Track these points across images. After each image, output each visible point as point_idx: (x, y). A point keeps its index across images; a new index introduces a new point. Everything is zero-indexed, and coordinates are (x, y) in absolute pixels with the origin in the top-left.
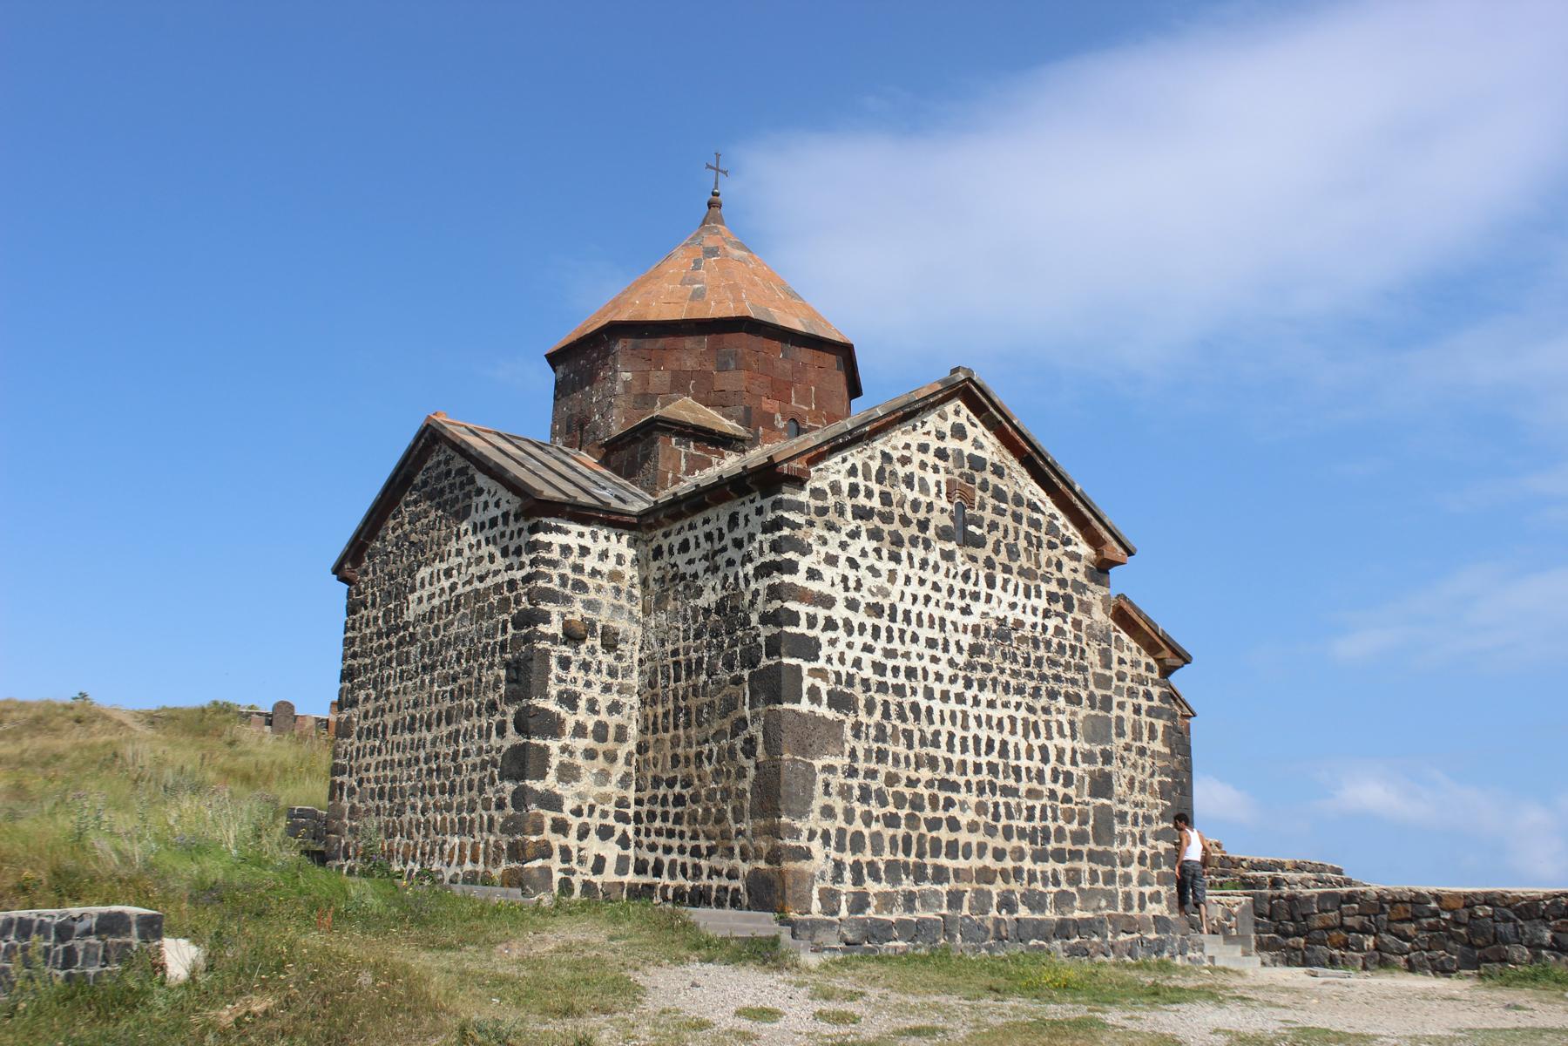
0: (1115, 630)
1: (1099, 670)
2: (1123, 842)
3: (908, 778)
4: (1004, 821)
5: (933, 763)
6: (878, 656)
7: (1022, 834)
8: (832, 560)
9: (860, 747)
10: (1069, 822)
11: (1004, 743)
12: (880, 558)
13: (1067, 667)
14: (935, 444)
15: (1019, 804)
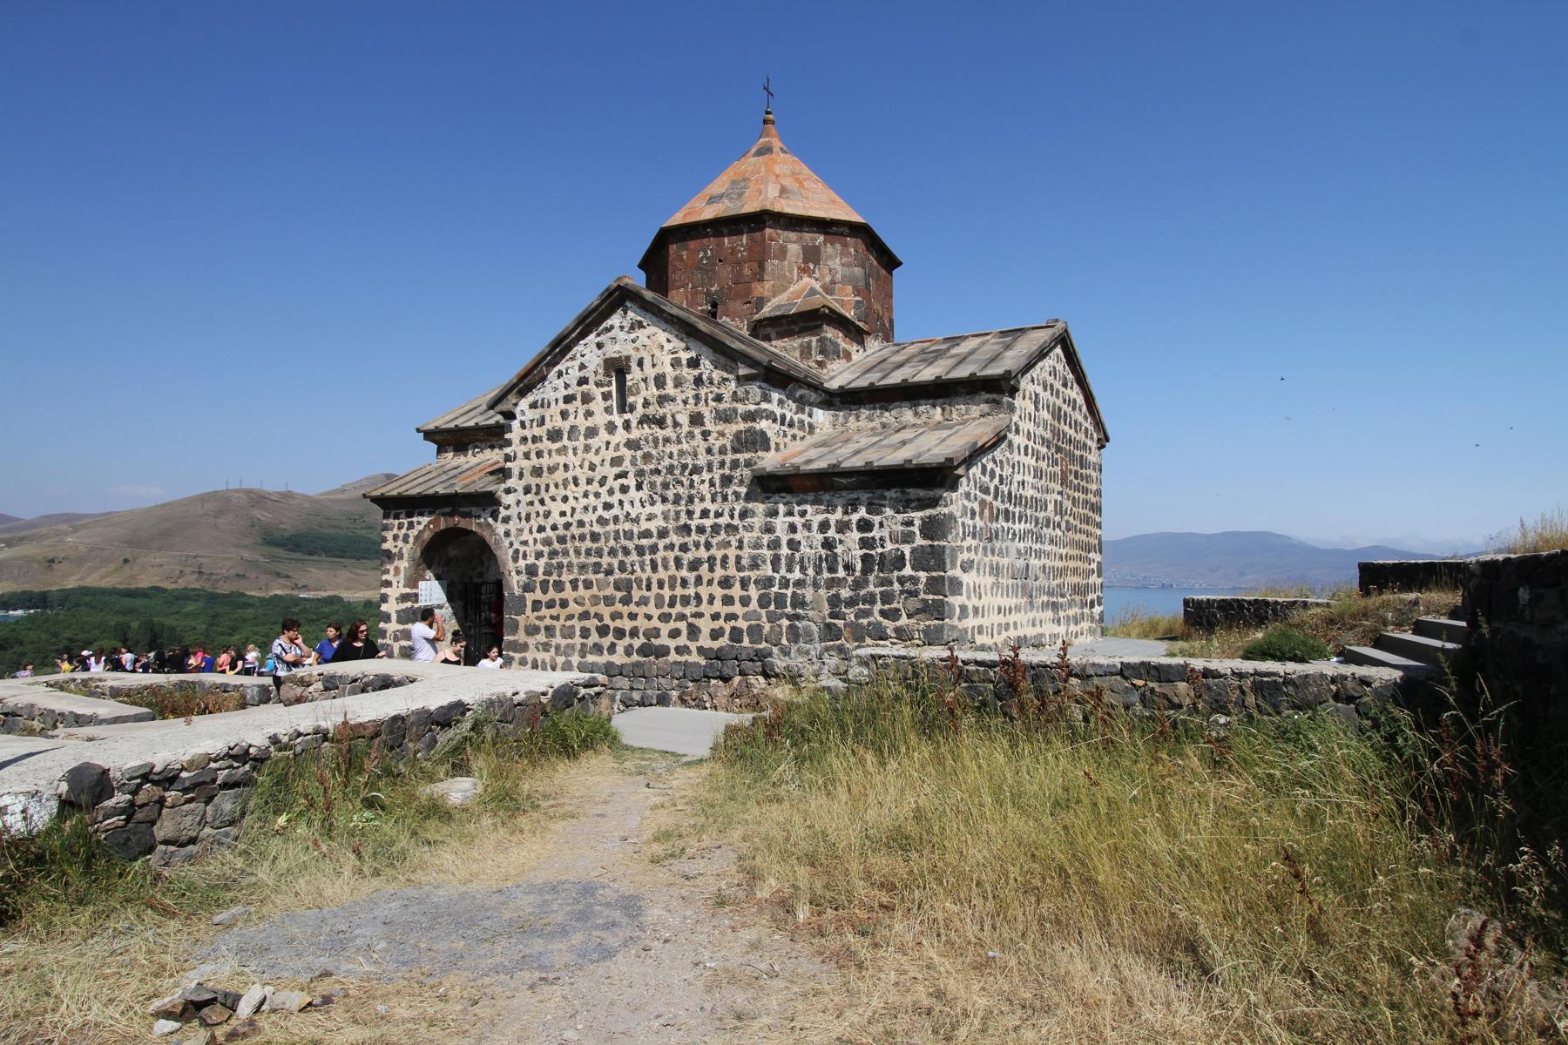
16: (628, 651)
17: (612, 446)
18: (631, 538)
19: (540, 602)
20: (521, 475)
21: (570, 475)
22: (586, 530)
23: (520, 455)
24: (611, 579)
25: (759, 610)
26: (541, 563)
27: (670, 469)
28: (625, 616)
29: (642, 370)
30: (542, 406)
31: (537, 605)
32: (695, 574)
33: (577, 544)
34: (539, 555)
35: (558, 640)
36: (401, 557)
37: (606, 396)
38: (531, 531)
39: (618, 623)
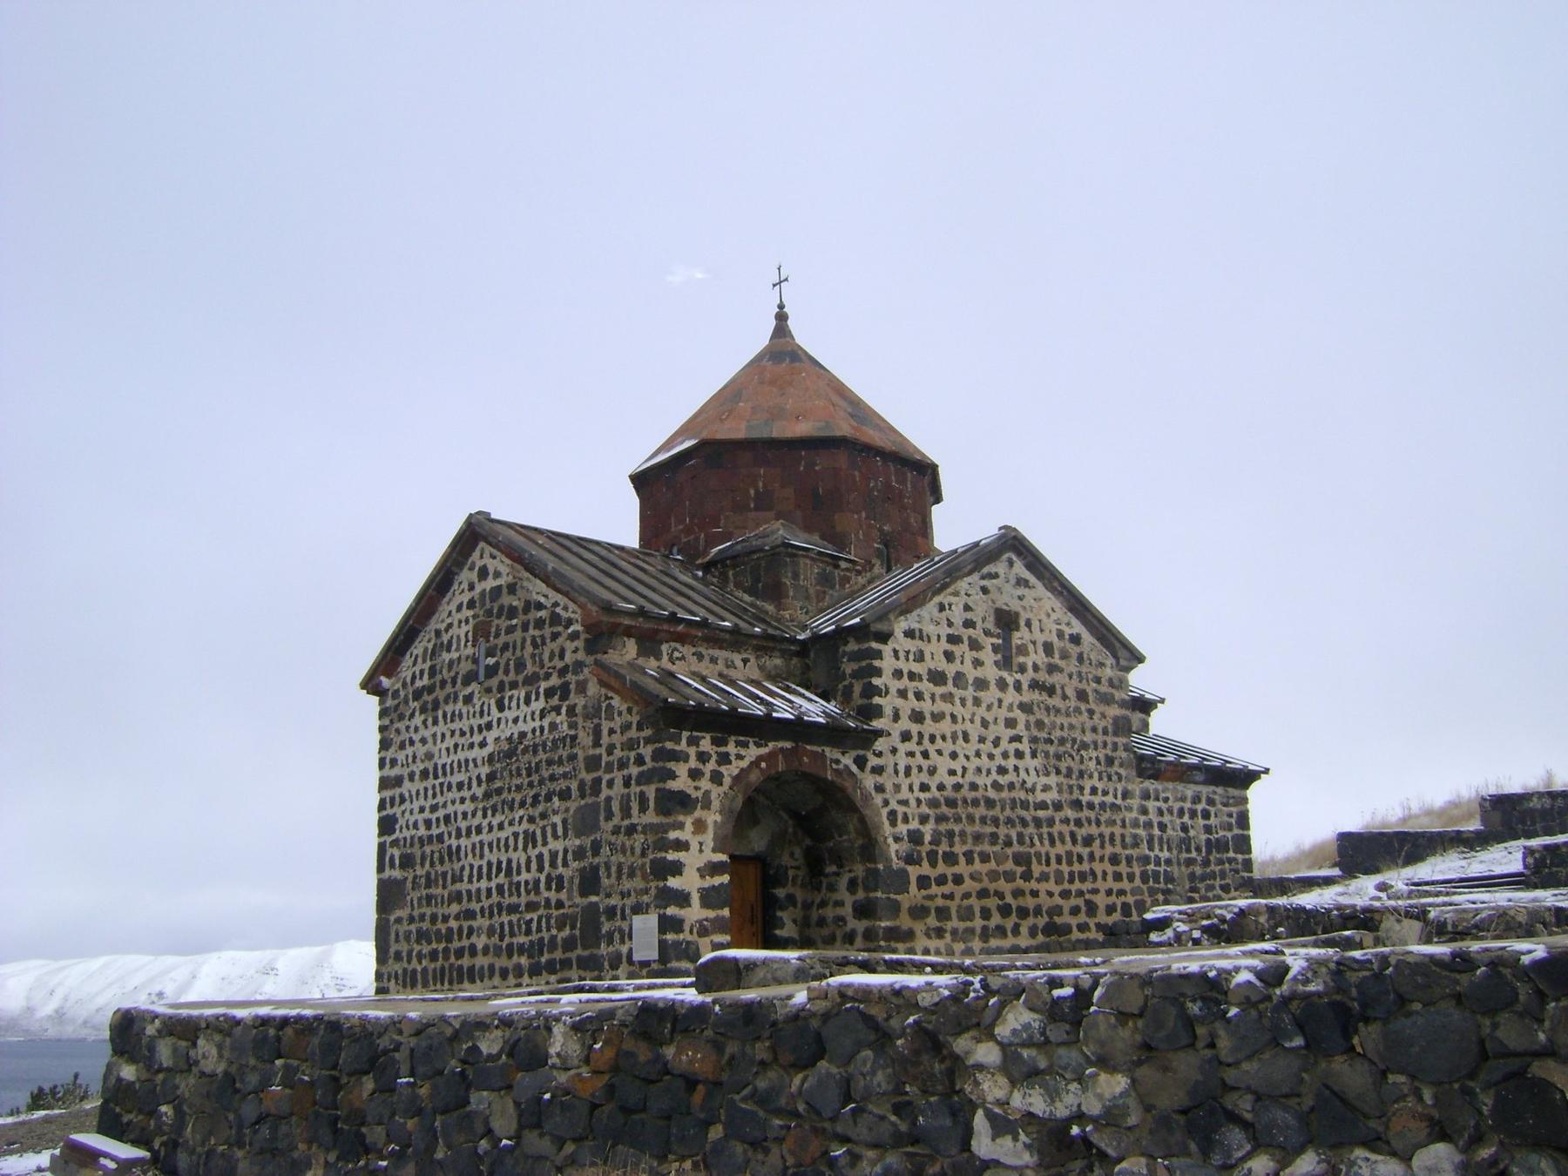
0: (607, 698)
1: (591, 752)
2: (610, 942)
3: (443, 915)
4: (507, 940)
5: (457, 897)
6: (427, 815)
7: (521, 950)
8: (402, 746)
9: (415, 895)
10: (560, 929)
11: (509, 861)
12: (426, 727)
13: (560, 762)
14: (466, 598)
15: (519, 920)
16: (1033, 932)
17: (1005, 704)
18: (1027, 809)
19: (928, 878)
20: (896, 717)
21: (959, 728)
22: (979, 794)
23: (893, 691)
24: (1009, 851)
25: (1141, 885)
26: (928, 830)
27: (1062, 741)
28: (1027, 892)
29: (1031, 632)
30: (921, 638)
31: (923, 882)
32: (1088, 850)
33: (970, 810)
34: (924, 819)
35: (955, 923)
36: (707, 805)
37: (995, 649)
38: (911, 789)
39: (1021, 902)
